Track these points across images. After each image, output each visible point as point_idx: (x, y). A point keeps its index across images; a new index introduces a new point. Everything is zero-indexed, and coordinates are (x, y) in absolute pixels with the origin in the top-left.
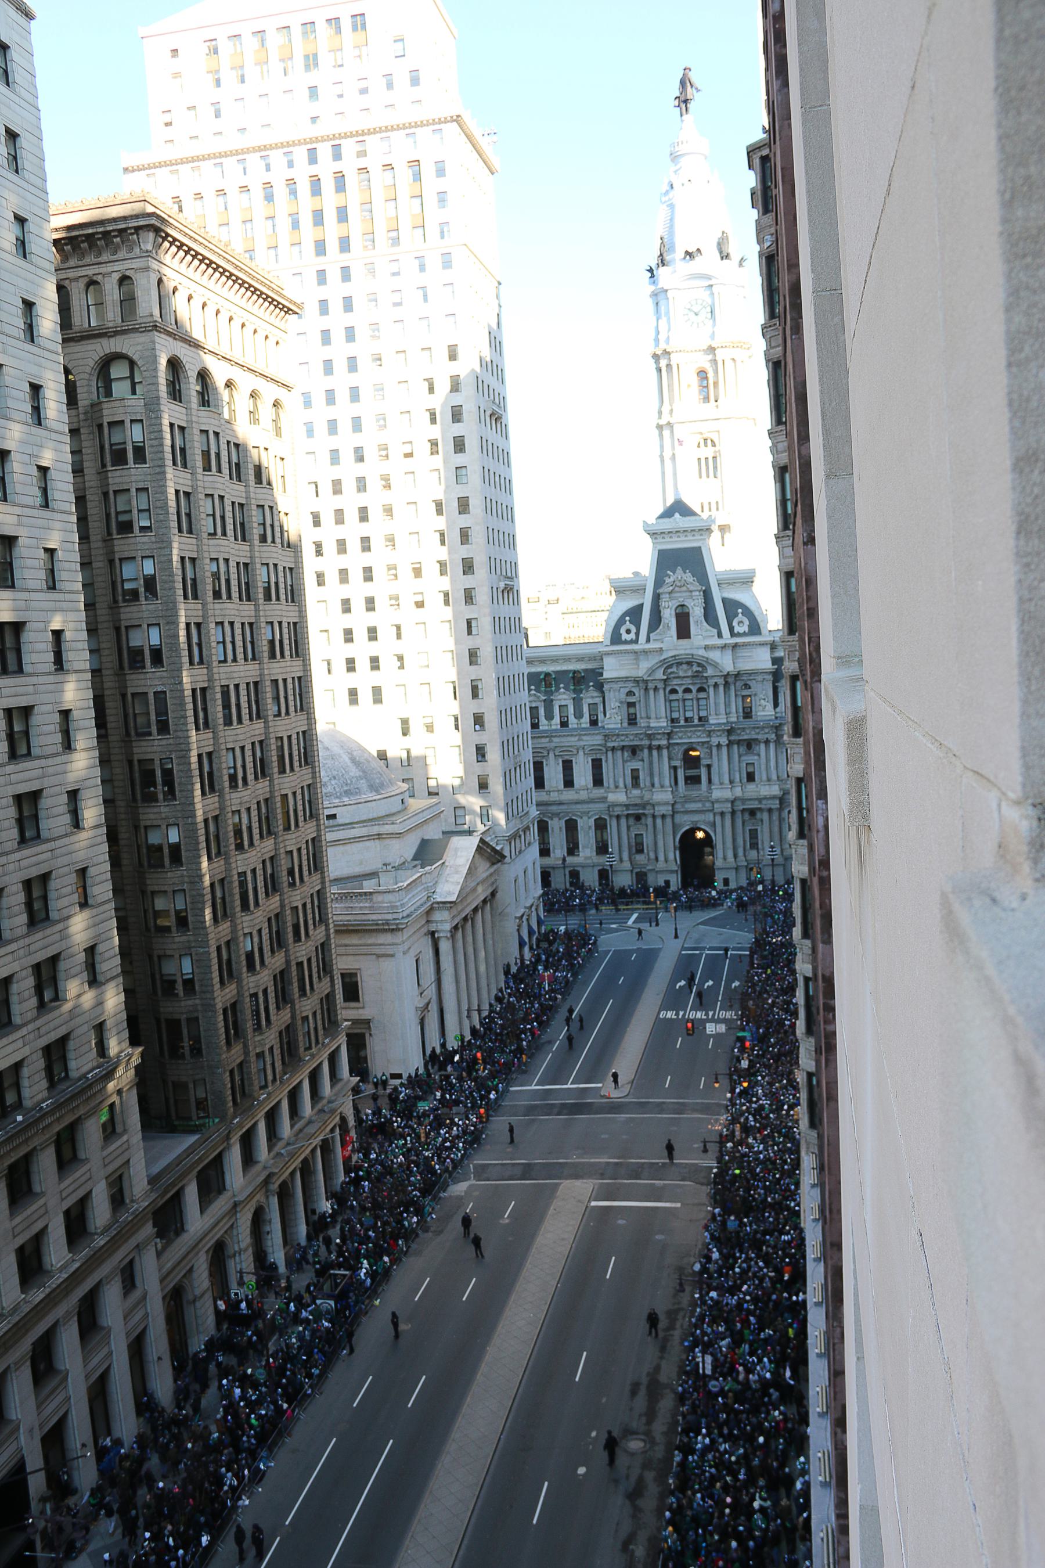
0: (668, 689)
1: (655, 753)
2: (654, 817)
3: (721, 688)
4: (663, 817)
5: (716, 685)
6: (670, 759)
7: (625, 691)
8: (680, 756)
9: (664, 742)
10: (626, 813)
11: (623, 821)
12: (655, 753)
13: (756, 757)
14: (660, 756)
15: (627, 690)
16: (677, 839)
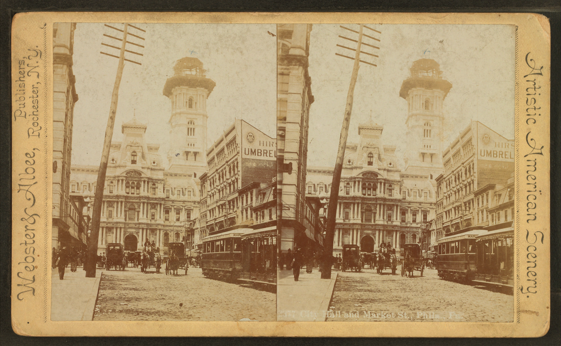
0: (127, 181)
1: (120, 204)
2: (117, 228)
3: (146, 182)
4: (121, 228)
5: (144, 181)
6: (125, 207)
7: (110, 181)
8: (128, 207)
9: (123, 200)
10: (106, 226)
11: (105, 229)
12: (120, 204)
13: (155, 210)
14: (121, 206)
15: (111, 181)
16: (125, 237)
